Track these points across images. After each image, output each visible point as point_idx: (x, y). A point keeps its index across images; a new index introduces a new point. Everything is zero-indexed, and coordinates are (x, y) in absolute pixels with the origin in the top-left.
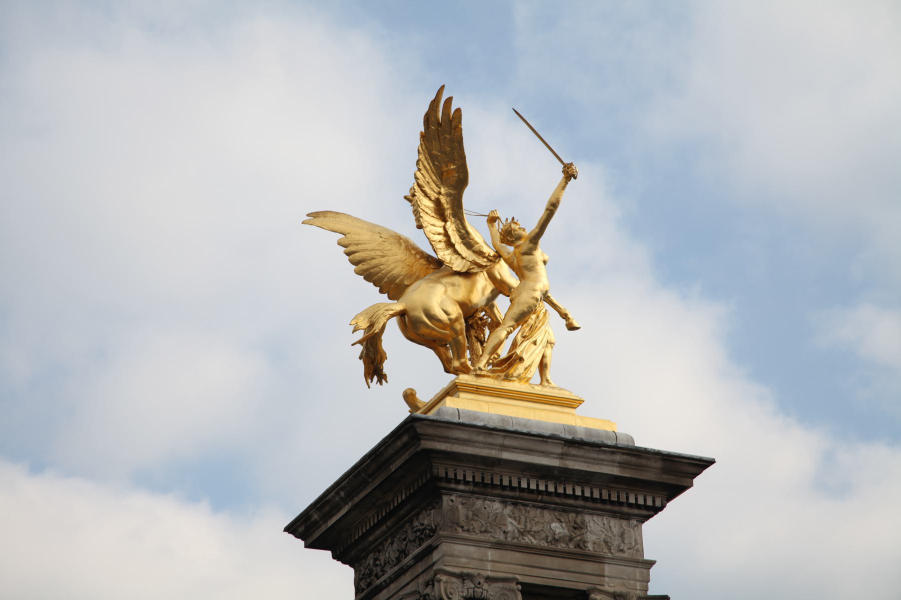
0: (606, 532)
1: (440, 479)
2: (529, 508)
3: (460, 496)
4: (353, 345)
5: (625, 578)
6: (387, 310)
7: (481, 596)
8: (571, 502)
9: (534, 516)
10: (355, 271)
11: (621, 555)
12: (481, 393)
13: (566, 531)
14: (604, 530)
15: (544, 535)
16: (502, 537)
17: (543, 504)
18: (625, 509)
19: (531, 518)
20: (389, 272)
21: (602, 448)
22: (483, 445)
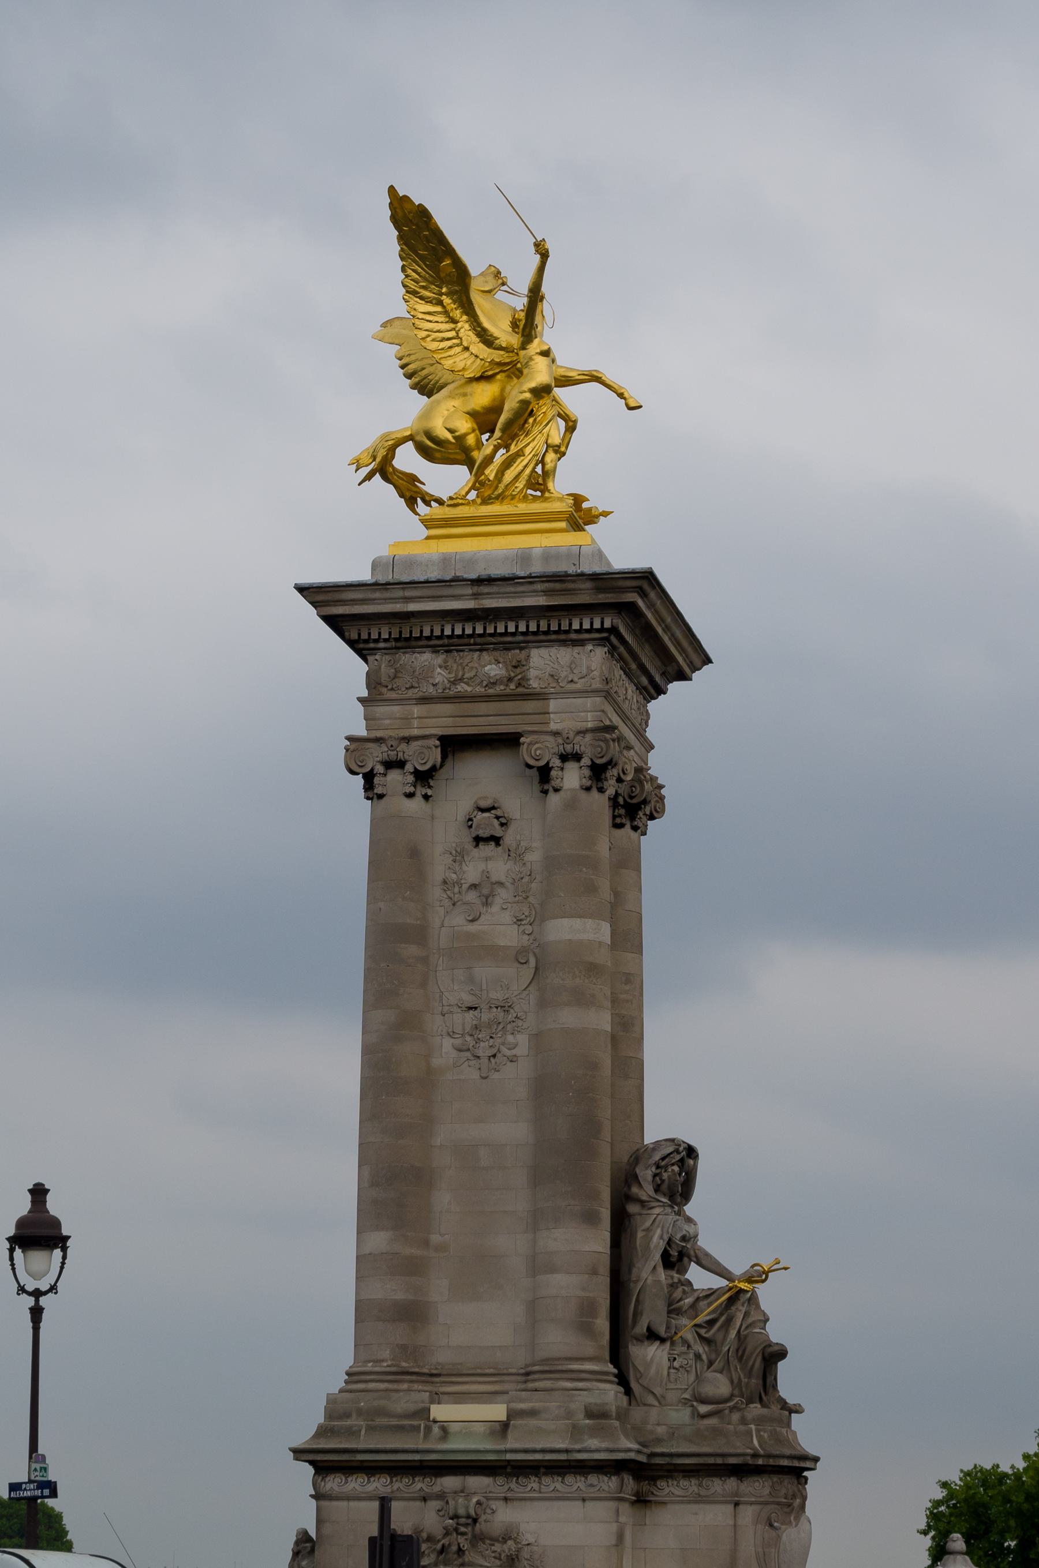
2: (466, 653)
3: (386, 654)
4: (359, 484)
5: (574, 711)
6: (387, 441)
7: (397, 758)
9: (469, 661)
10: (411, 388)
12: (456, 525)
15: (479, 680)
19: (464, 664)
20: (437, 382)
21: (516, 581)
22: (384, 601)
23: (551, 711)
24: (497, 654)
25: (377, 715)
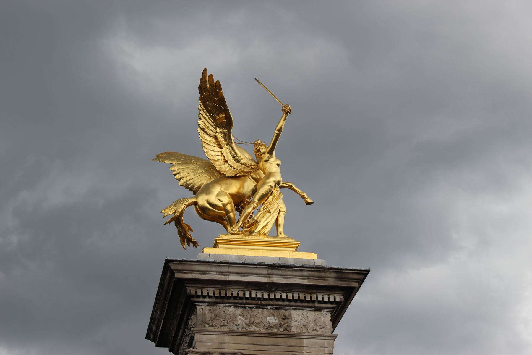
0: (305, 320)
1: (193, 296)
2: (254, 309)
3: (208, 306)
4: (164, 225)
8: (280, 303)
9: (256, 314)
11: (315, 332)
13: (277, 321)
14: (303, 319)
15: (262, 325)
16: (235, 328)
17: (263, 306)
18: (317, 305)
19: (254, 315)
23: (304, 345)
24: (272, 311)
25: (203, 339)
